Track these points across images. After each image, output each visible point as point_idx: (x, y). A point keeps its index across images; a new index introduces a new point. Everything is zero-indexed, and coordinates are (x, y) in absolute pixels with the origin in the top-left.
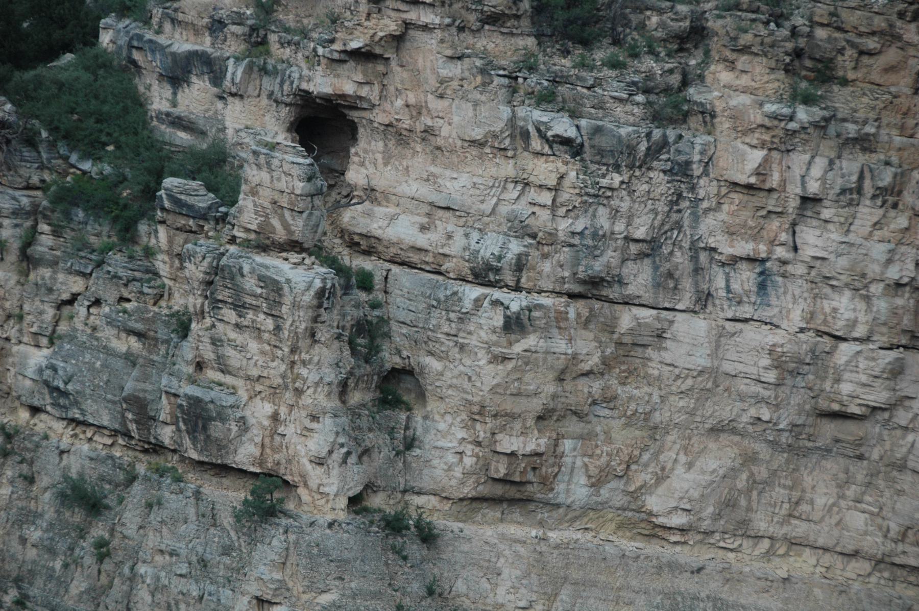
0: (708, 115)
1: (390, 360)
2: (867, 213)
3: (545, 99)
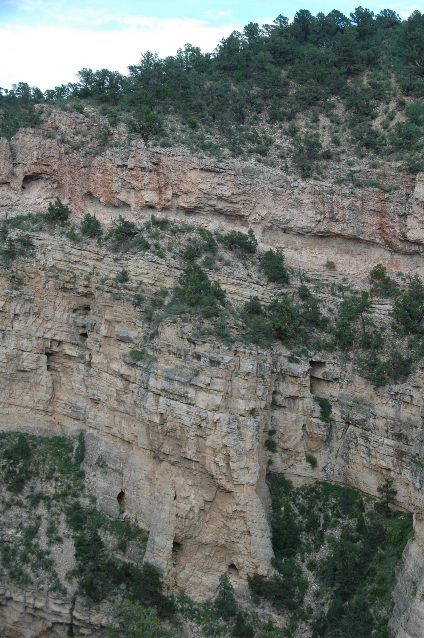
2: (31, 319)
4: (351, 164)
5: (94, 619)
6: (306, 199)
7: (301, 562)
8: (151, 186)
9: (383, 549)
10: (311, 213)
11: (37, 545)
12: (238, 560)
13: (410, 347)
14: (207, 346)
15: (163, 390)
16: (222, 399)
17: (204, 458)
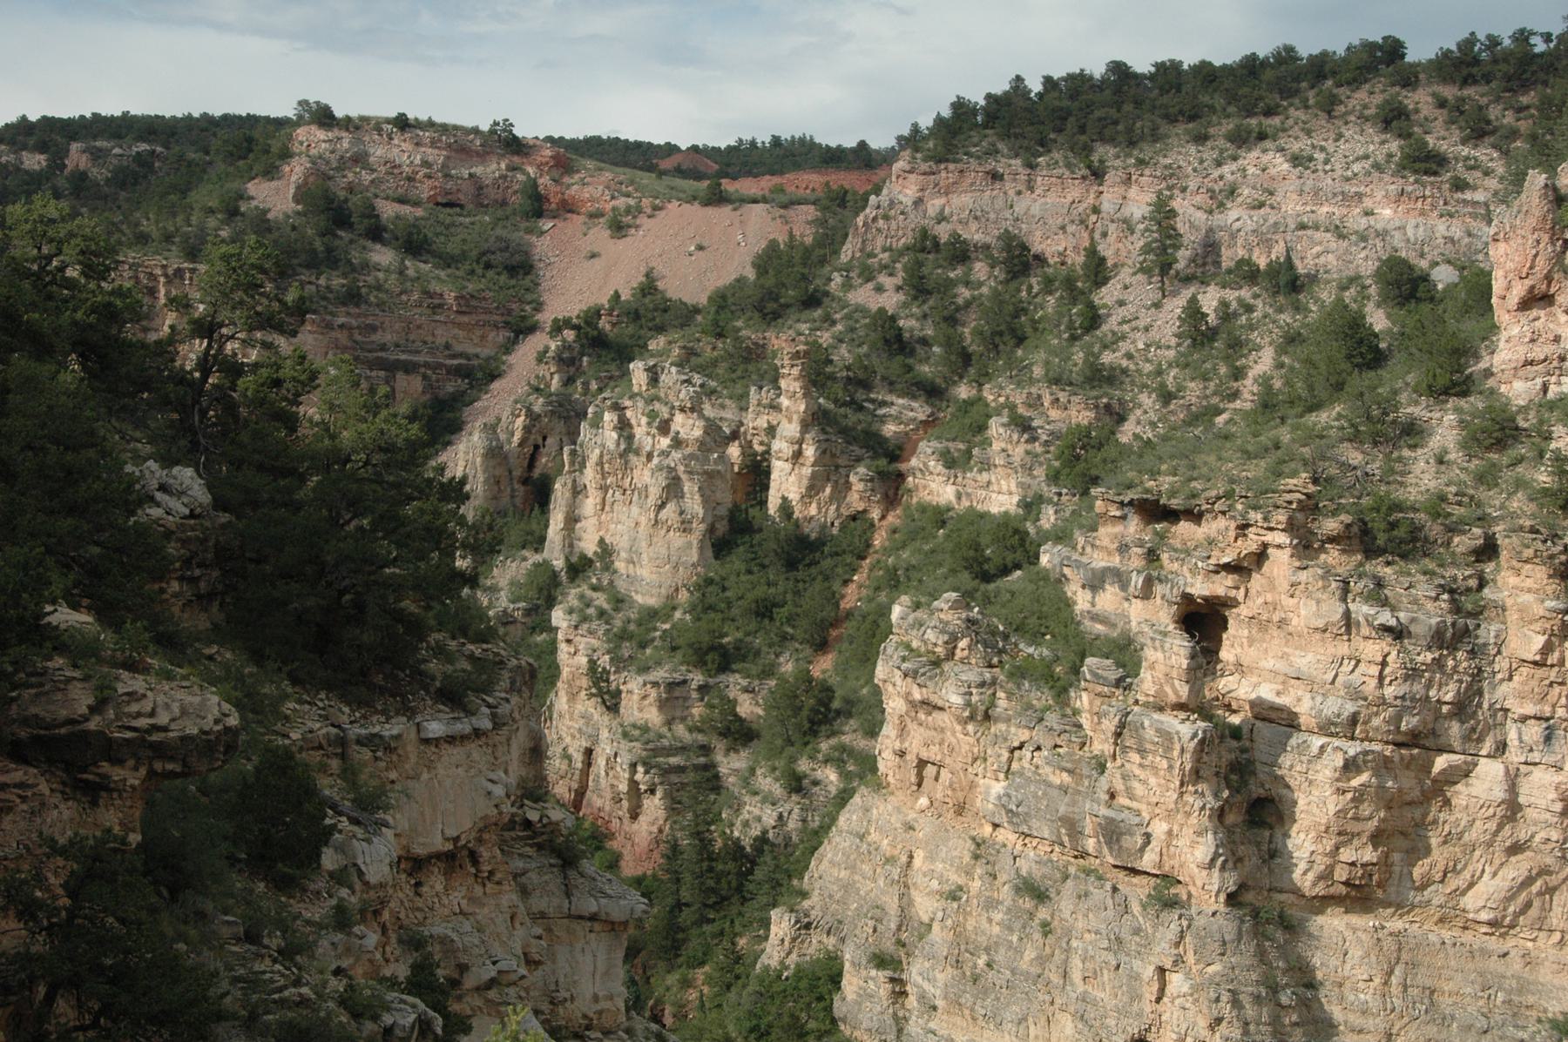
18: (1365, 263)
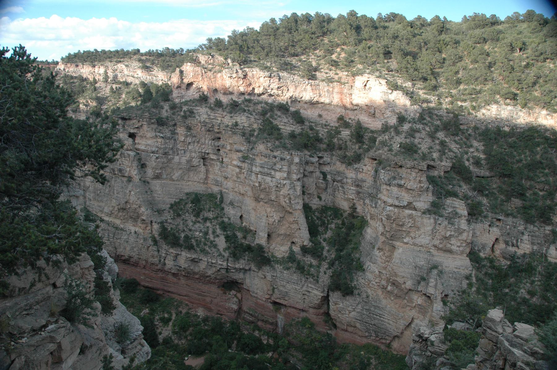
0: (178, 134)
1: (142, 163)
2: (196, 144)
3: (159, 132)
4: (327, 73)
5: (237, 266)
6: (309, 87)
7: (320, 239)
8: (243, 85)
9: (354, 231)
10: (311, 94)
11: (209, 238)
12: (295, 240)
13: (360, 148)
14: (279, 152)
15: (260, 172)
16: (282, 175)
17: (280, 199)
18: (137, 82)
